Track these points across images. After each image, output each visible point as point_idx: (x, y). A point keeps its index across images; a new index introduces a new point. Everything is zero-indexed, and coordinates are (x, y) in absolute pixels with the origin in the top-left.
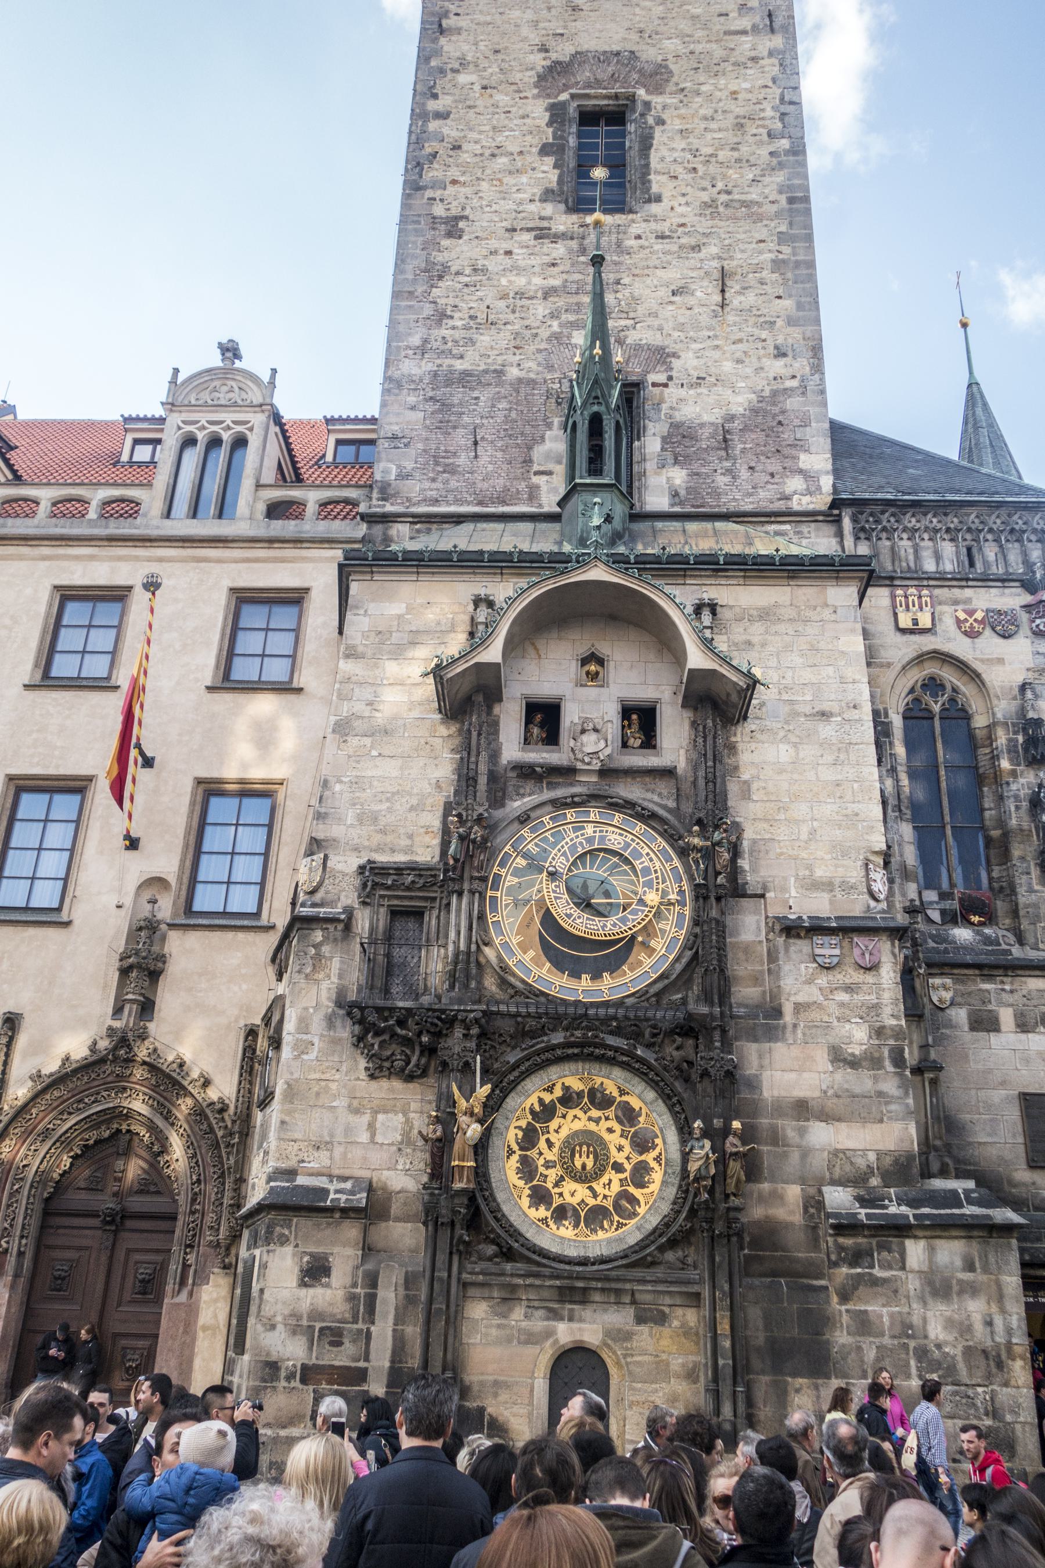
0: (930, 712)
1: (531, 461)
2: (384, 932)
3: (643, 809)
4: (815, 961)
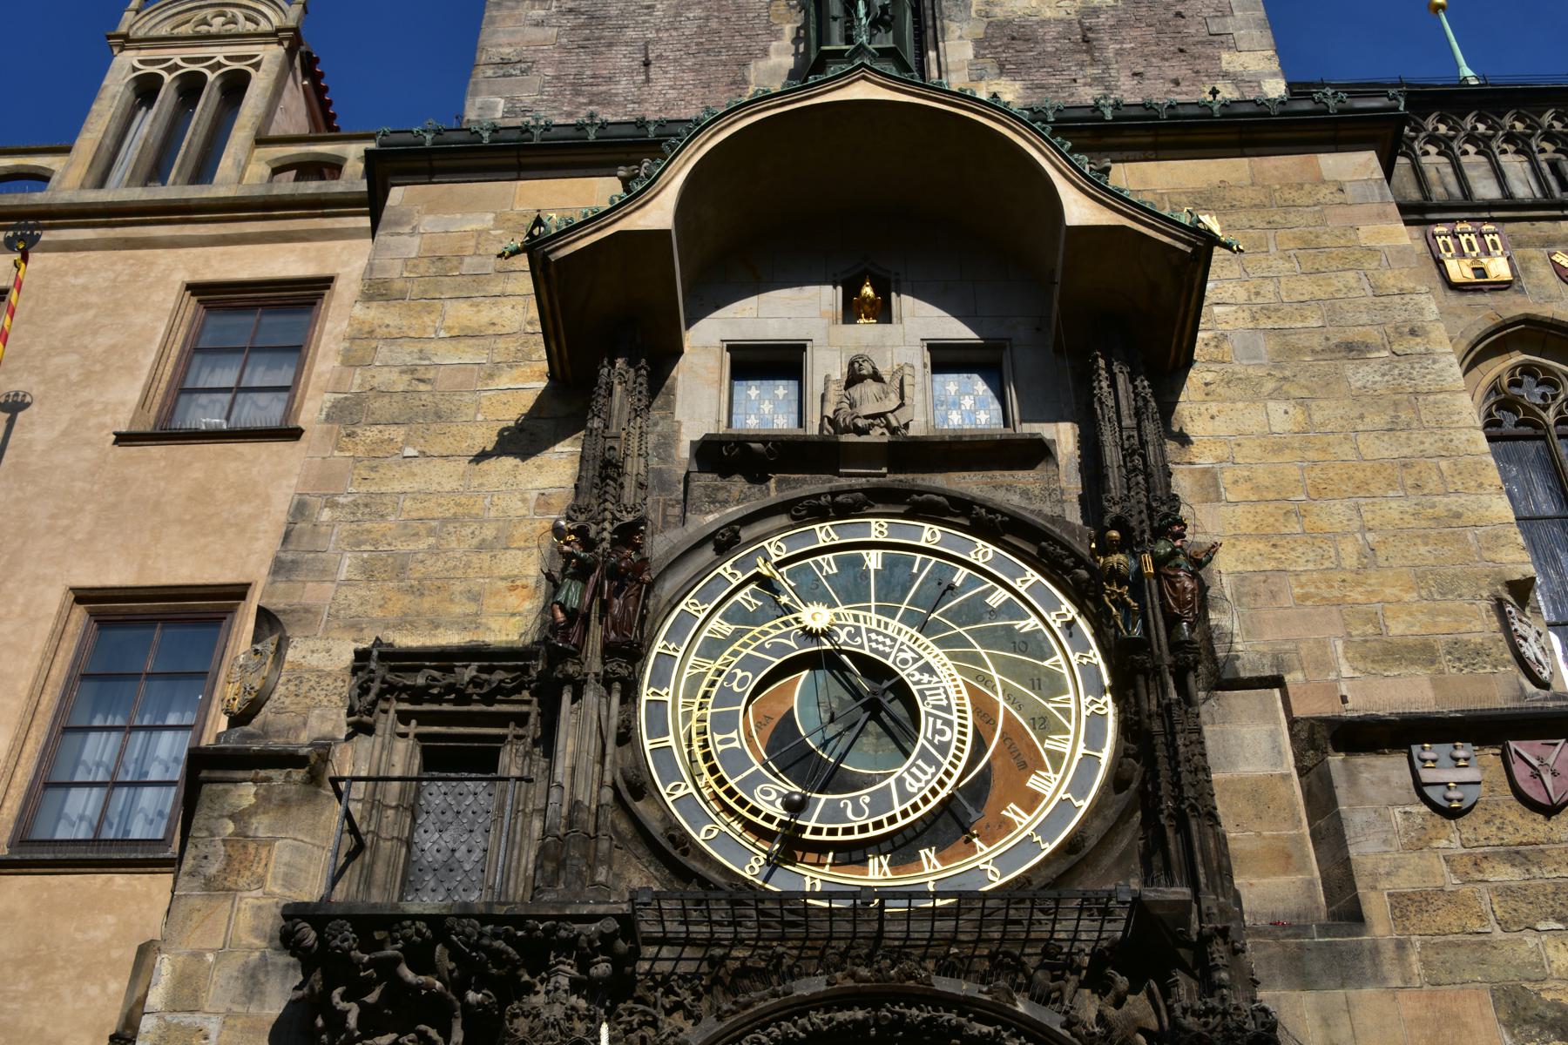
0: (1536, 426)
1: (745, 82)
2: (402, 792)
3: (990, 510)
4: (1426, 800)
